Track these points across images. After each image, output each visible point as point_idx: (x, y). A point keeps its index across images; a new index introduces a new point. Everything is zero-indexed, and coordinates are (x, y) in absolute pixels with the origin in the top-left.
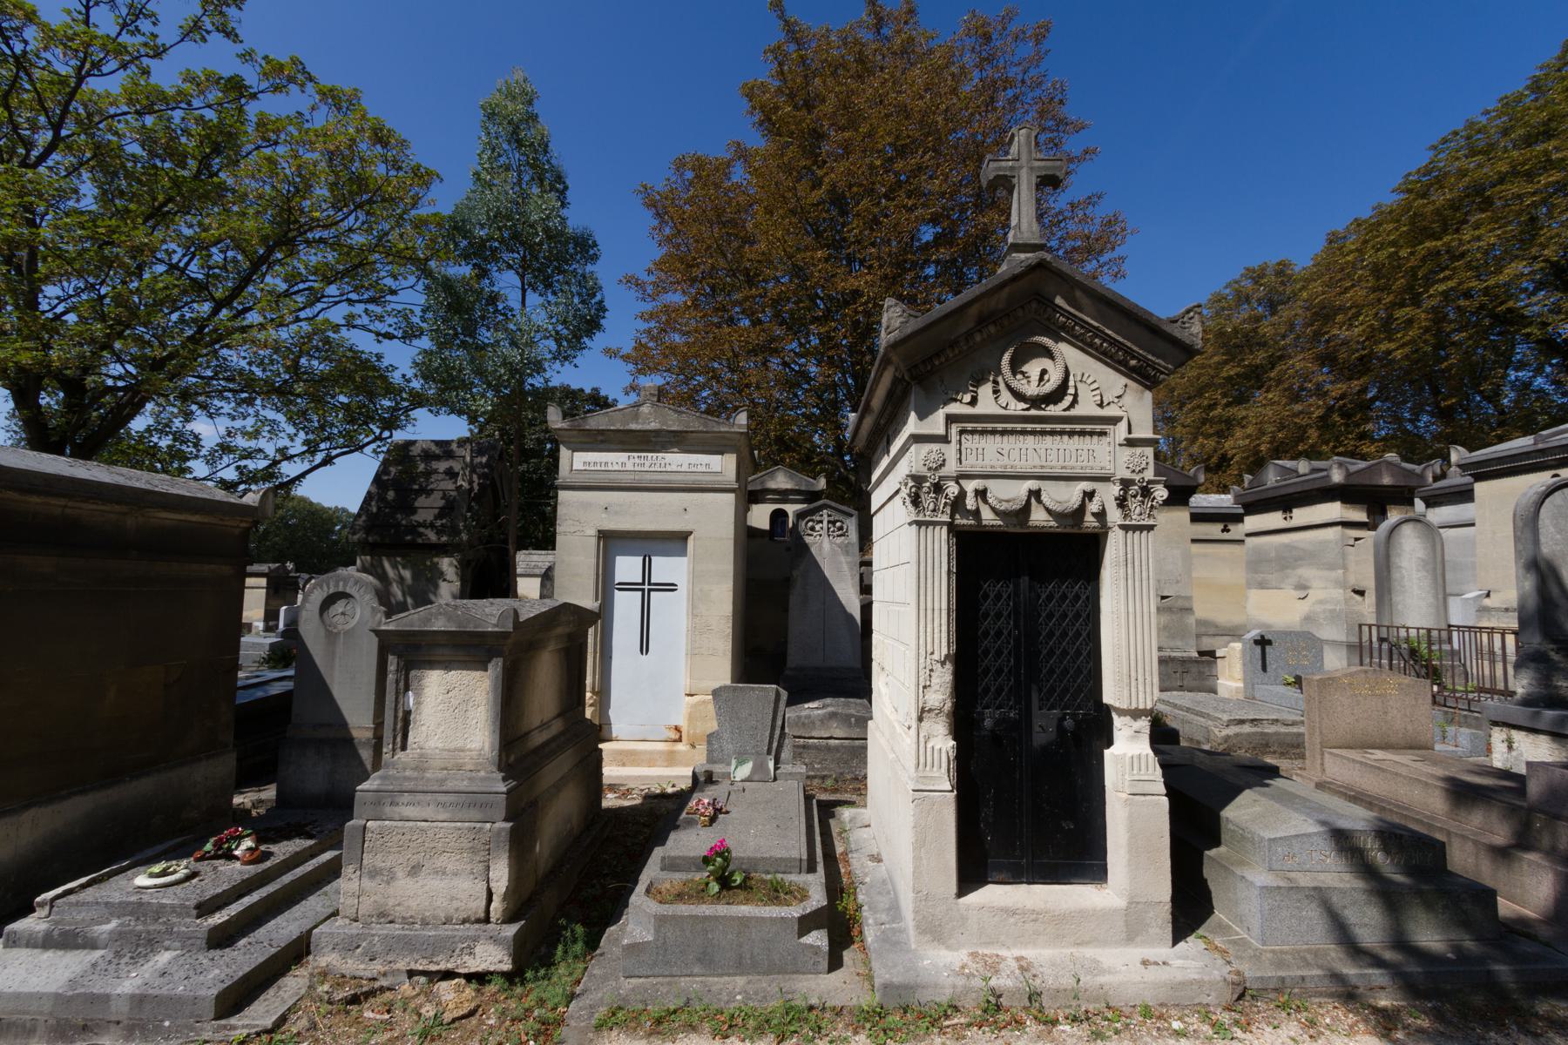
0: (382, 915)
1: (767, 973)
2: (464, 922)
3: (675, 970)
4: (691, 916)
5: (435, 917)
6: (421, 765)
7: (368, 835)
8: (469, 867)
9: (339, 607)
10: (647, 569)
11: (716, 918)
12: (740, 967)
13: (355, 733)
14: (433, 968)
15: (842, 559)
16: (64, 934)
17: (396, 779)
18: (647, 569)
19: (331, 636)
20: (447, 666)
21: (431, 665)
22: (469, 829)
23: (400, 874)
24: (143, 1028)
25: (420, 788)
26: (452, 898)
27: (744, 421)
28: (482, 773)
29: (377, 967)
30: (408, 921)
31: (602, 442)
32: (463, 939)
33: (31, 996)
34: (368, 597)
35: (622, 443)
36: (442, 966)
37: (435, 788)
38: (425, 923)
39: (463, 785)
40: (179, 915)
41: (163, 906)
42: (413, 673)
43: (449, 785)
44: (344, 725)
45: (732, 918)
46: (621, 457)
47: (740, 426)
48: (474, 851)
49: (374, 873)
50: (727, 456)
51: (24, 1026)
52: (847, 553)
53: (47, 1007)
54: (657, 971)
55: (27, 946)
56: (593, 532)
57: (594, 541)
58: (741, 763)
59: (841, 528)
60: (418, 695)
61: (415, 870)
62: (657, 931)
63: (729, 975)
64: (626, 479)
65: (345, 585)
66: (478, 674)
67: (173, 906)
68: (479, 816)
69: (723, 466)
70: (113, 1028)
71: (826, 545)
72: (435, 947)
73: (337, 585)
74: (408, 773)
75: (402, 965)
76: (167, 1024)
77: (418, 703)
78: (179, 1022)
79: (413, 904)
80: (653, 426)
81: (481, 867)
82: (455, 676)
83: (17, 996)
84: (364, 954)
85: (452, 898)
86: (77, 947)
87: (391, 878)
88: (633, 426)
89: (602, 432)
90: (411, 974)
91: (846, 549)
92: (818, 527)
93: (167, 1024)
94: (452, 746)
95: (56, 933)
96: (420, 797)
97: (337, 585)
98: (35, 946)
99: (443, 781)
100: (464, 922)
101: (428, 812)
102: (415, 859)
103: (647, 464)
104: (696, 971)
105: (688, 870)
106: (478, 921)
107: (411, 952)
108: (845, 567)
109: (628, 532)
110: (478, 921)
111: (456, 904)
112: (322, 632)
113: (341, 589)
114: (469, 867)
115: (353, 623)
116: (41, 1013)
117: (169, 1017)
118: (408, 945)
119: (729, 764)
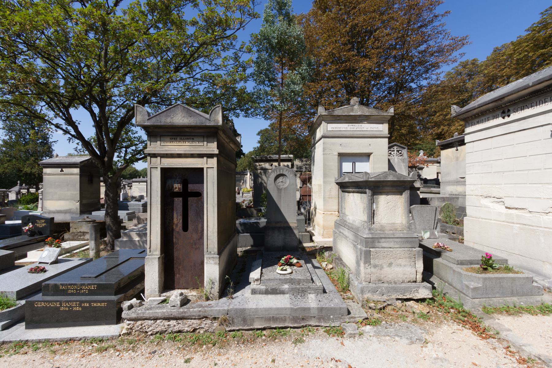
0: (380, 280)
1: (522, 295)
2: (409, 282)
3: (490, 296)
4: (495, 278)
5: (398, 281)
6: (382, 228)
7: (372, 253)
8: (409, 263)
9: (280, 179)
10: (354, 167)
11: (504, 278)
12: (512, 294)
13: (291, 225)
14: (405, 297)
15: (402, 164)
16: (272, 289)
17: (376, 234)
18: (354, 167)
19: (279, 190)
20: (387, 193)
21: (381, 193)
22: (408, 250)
23: (385, 266)
24: (324, 319)
25: (387, 237)
26: (404, 274)
27: (393, 111)
28: (405, 231)
29: (385, 298)
30: (389, 282)
31: (338, 120)
32: (414, 288)
33: (282, 309)
34: (291, 175)
35: (346, 120)
36: (408, 297)
37: (392, 236)
38: (395, 283)
39: (402, 235)
40: (306, 282)
41: (300, 280)
42: (375, 196)
43: (397, 236)
44: (286, 222)
45: (510, 278)
46: (346, 125)
47: (391, 113)
48: (410, 258)
49: (375, 266)
50: (384, 124)
51: (282, 319)
52: (404, 162)
53: (289, 313)
54: (483, 296)
55: (260, 294)
56: (337, 154)
57: (337, 156)
58: (426, 232)
59: (401, 153)
60: (377, 204)
61: (390, 265)
62: (483, 283)
63: (509, 297)
64: (348, 134)
65: (283, 171)
66: (398, 196)
67: (304, 280)
68: (410, 246)
69: (384, 128)
70: (313, 319)
71: (396, 160)
72: (405, 290)
73: (280, 171)
74: (379, 232)
75: (394, 296)
76: (332, 317)
77: (377, 207)
78: (336, 316)
79: (390, 276)
80: (359, 113)
81: (413, 263)
82: (391, 198)
83: (278, 309)
84: (380, 293)
85: (404, 274)
86: (278, 294)
87: (382, 268)
88: (352, 114)
89: (339, 116)
90: (398, 299)
91: (403, 161)
92: (392, 153)
93: (332, 317)
94: (390, 222)
95: (269, 289)
96: (388, 240)
97: (280, 171)
98: (262, 294)
99: (393, 234)
100: (409, 282)
101: (391, 245)
102: (389, 261)
103: (355, 128)
104: (497, 296)
105: (467, 265)
106: (414, 282)
107: (396, 292)
108: (403, 167)
109: (349, 154)
110: (414, 282)
111: (405, 276)
112: (276, 189)
113: (278, 173)
114: (409, 263)
115: (286, 186)
116: (287, 314)
117: (332, 315)
118: (395, 290)
119: (421, 233)
